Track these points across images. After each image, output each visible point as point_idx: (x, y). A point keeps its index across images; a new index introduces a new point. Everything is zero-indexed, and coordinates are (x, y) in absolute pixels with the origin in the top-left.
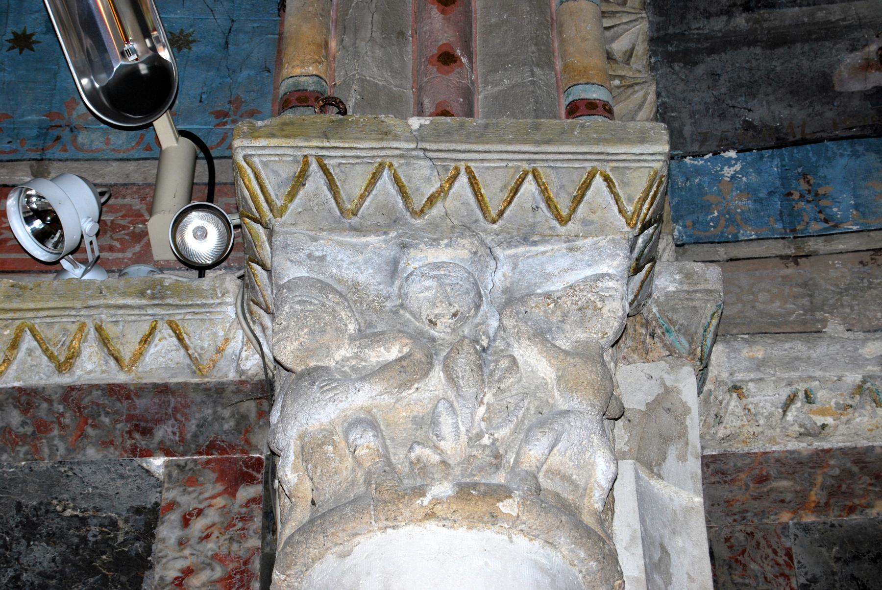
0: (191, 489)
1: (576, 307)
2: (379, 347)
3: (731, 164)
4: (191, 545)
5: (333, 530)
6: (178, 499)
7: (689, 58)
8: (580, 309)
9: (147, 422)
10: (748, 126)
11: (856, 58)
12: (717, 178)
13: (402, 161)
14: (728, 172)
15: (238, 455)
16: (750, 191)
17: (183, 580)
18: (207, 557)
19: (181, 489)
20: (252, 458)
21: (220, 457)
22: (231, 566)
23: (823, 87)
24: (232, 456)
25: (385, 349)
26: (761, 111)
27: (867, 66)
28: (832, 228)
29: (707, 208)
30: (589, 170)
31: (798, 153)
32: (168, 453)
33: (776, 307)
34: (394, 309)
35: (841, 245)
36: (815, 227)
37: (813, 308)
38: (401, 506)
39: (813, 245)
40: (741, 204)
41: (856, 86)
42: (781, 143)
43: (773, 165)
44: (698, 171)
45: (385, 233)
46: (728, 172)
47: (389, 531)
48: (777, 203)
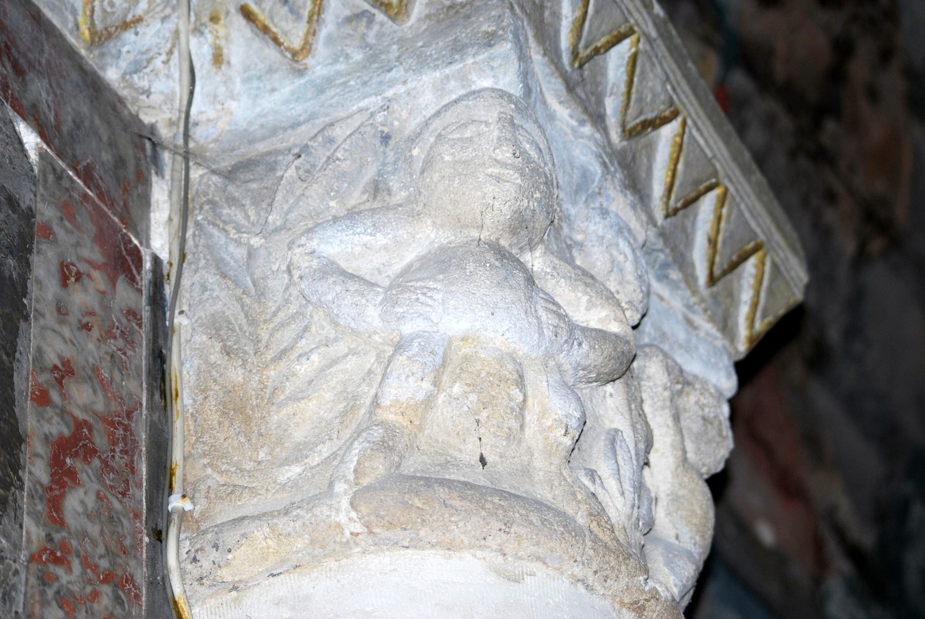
0: (67, 224)
1: (700, 413)
2: (586, 293)
4: (70, 324)
5: (522, 531)
6: (56, 228)
8: (704, 419)
9: (19, 53)
13: (648, 47)
15: (116, 219)
17: (63, 377)
18: (88, 362)
19: (59, 214)
20: (130, 241)
21: (96, 199)
22: (114, 406)
24: (109, 213)
25: (590, 301)
30: (758, 241)
32: (42, 135)
34: (569, 242)
38: (623, 568)
45: (582, 123)
47: (581, 588)
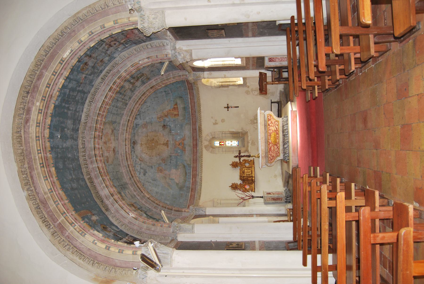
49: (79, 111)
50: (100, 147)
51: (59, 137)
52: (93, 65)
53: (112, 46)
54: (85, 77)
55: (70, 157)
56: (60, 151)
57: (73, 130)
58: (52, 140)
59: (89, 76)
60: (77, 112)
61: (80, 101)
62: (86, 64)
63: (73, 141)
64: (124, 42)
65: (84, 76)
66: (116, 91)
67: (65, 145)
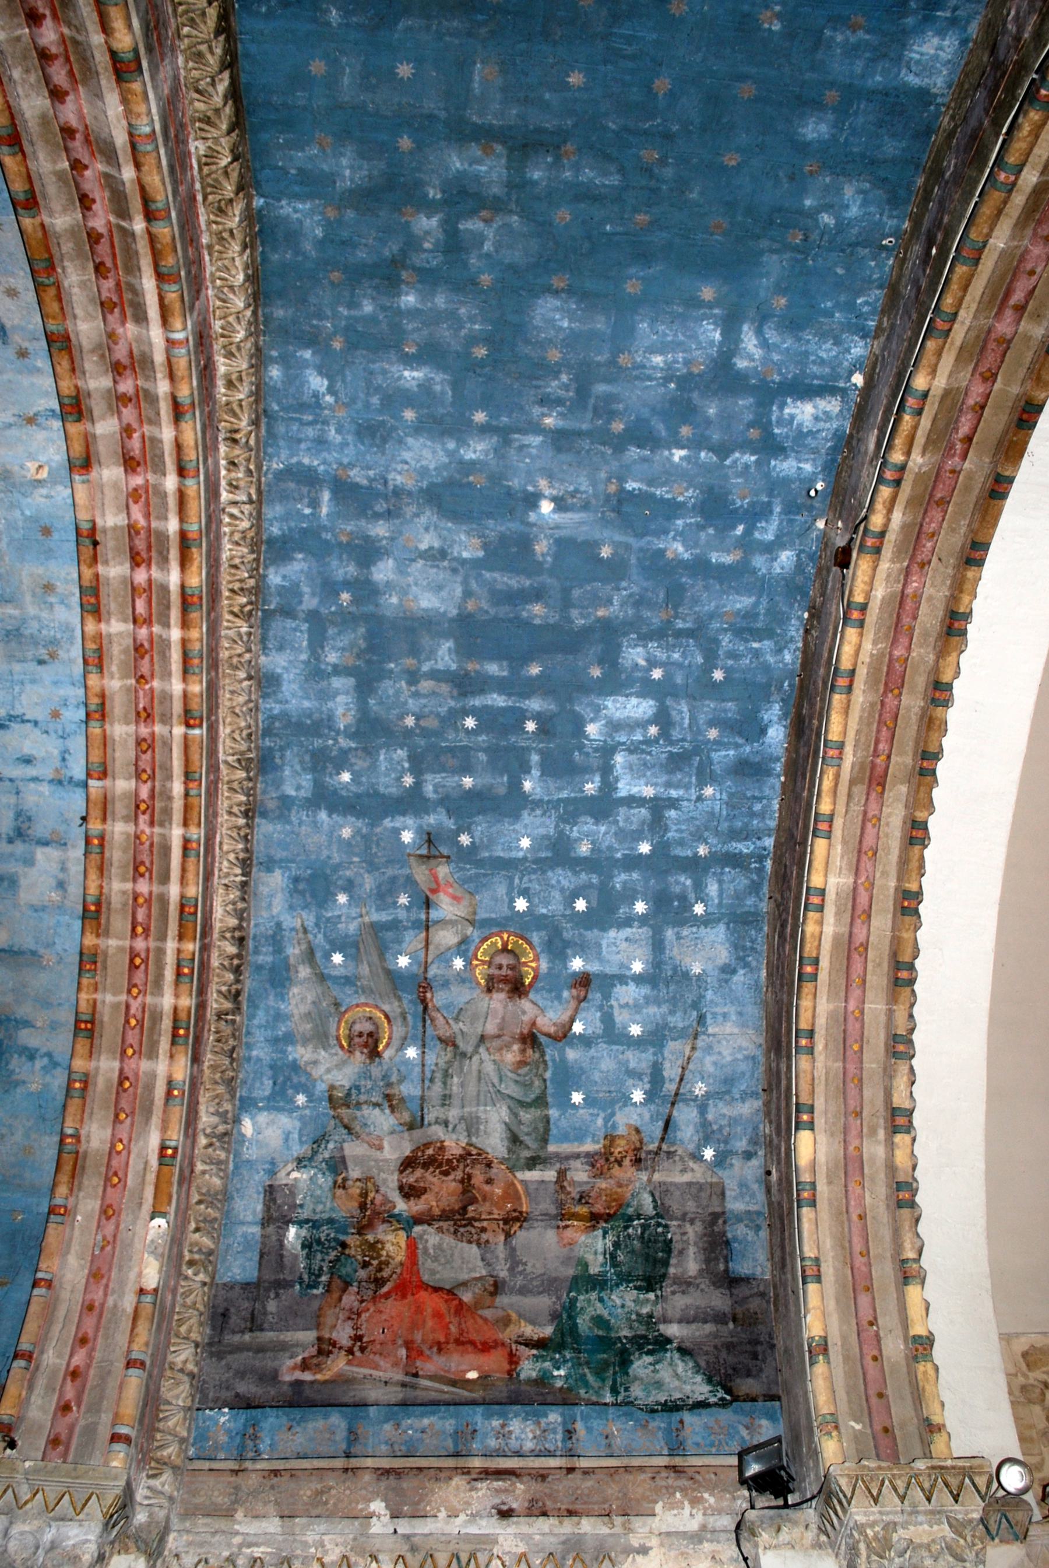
3: (224, 1417)
7: (219, 1356)
10: (237, 1395)
11: (290, 1363)
12: (217, 1423)
14: (222, 1419)
16: (228, 1431)
23: (273, 1377)
26: (243, 1388)
27: (294, 1368)
28: (257, 1457)
29: (208, 1439)
31: (254, 1412)
33: (219, 1500)
35: (259, 1466)
36: (251, 1455)
37: (236, 1502)
39: (248, 1464)
40: (223, 1438)
41: (288, 1378)
42: (249, 1407)
43: (243, 1415)
44: (210, 1418)
46: (222, 1419)
48: (238, 1440)
49: (315, 673)
50: (110, 473)
51: (546, 507)
52: (438, 998)
53: (408, 1164)
54: (428, 904)
55: (408, 361)
56: (537, 410)
57: (367, 552)
58: (631, 485)
59: (375, 917)
60: (337, 670)
61: (344, 742)
62: (517, 988)
63: (356, 475)
64: (374, 1247)
65: (446, 908)
66: (120, 923)
67: (476, 450)
